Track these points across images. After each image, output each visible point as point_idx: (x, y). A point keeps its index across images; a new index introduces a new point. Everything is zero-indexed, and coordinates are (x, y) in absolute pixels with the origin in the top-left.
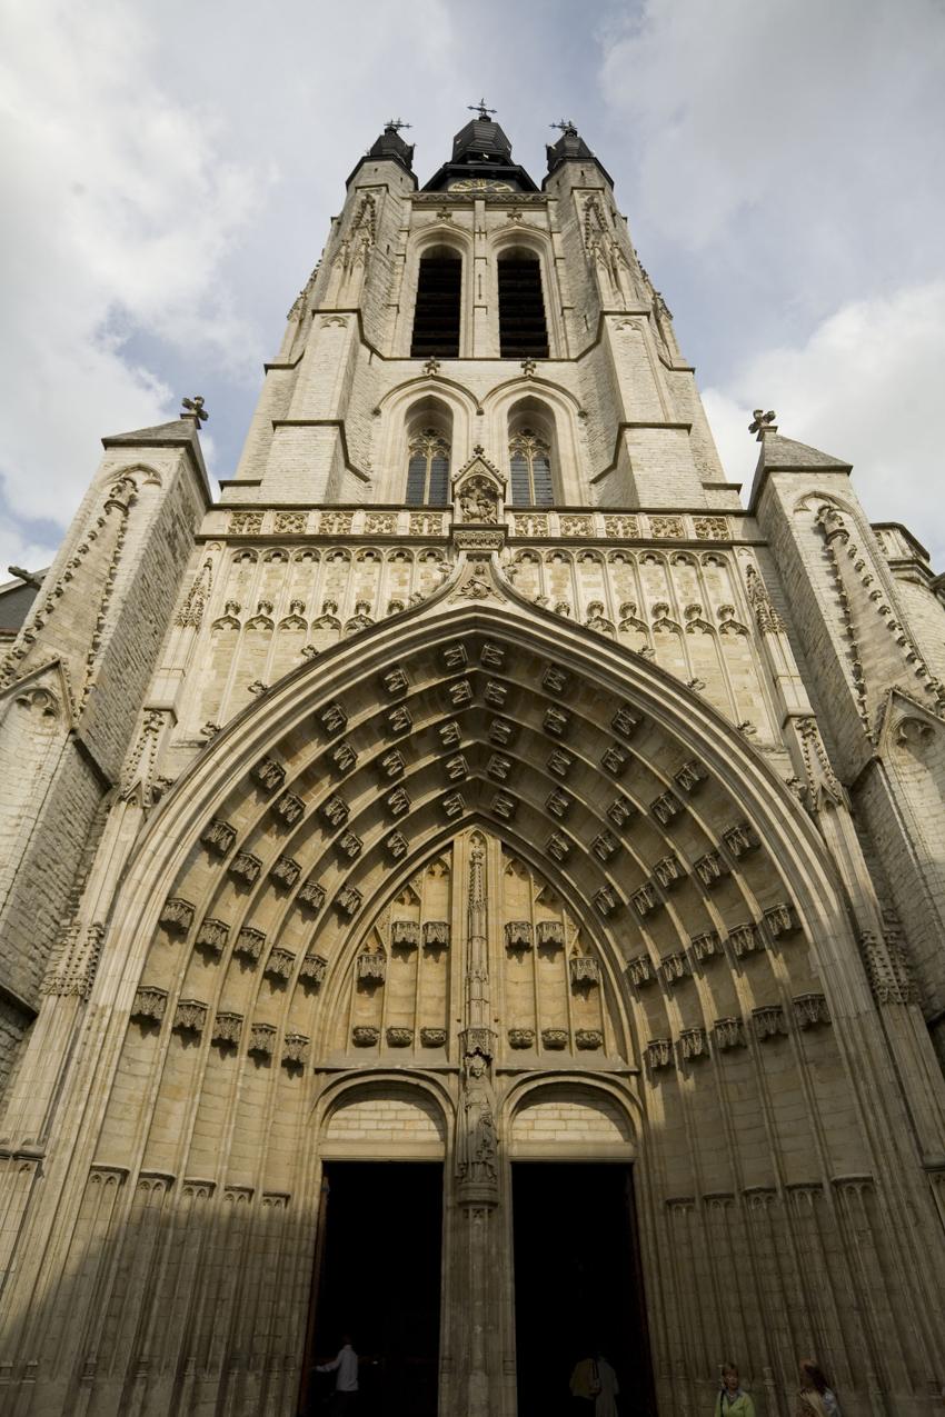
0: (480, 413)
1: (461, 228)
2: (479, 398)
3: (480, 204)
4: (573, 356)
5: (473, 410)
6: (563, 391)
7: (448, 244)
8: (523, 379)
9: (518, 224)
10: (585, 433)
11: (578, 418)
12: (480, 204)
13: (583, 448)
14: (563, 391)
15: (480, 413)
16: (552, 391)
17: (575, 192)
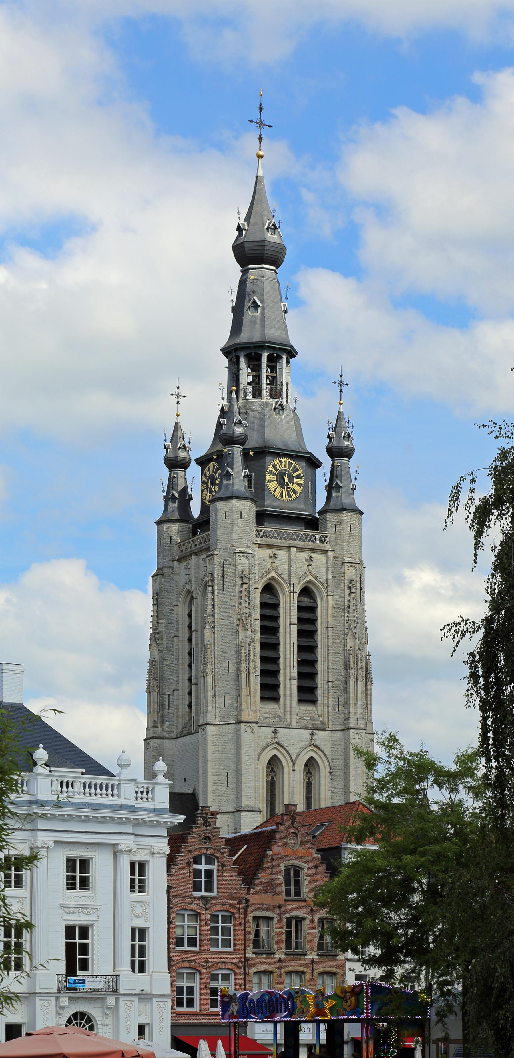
0: (294, 770)
1: (283, 579)
2: (294, 759)
3: (293, 550)
4: (331, 727)
5: (291, 768)
6: (325, 755)
7: (273, 582)
8: (310, 746)
9: (312, 575)
10: (330, 785)
11: (328, 774)
12: (293, 550)
13: (329, 794)
14: (325, 755)
15: (294, 770)
16: (320, 753)
17: (346, 564)
